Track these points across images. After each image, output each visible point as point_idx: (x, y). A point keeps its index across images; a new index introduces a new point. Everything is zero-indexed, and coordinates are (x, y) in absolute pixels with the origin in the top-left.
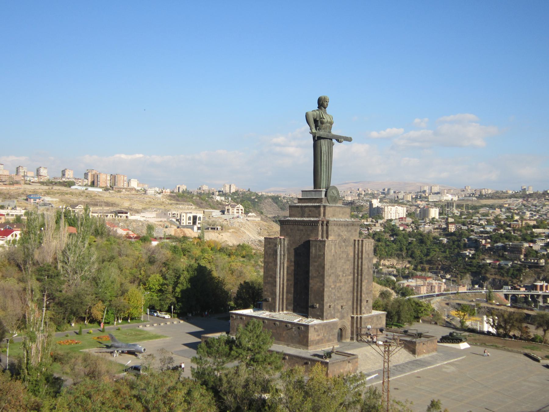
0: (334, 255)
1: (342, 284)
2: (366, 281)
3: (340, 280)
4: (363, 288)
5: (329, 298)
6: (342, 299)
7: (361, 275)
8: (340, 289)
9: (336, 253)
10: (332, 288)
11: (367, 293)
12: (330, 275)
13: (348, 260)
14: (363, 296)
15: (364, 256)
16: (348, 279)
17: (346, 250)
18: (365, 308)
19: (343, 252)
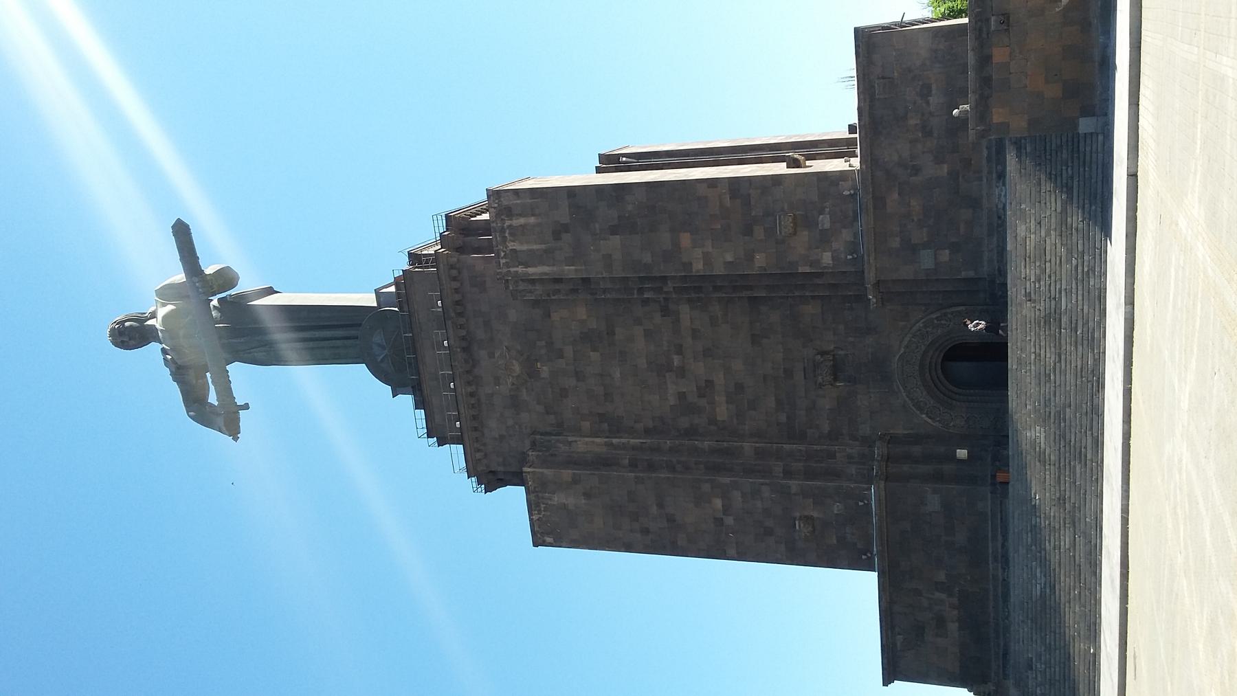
0: (587, 495)
1: (719, 379)
2: (685, 239)
3: (701, 396)
4: (719, 270)
5: (769, 532)
6: (789, 373)
7: (664, 279)
8: (740, 387)
9: (576, 481)
10: (726, 510)
11: (748, 231)
12: (671, 519)
13: (611, 333)
14: (760, 259)
15: (569, 271)
16: (695, 334)
17: (569, 351)
18: (824, 239)
19: (579, 376)
